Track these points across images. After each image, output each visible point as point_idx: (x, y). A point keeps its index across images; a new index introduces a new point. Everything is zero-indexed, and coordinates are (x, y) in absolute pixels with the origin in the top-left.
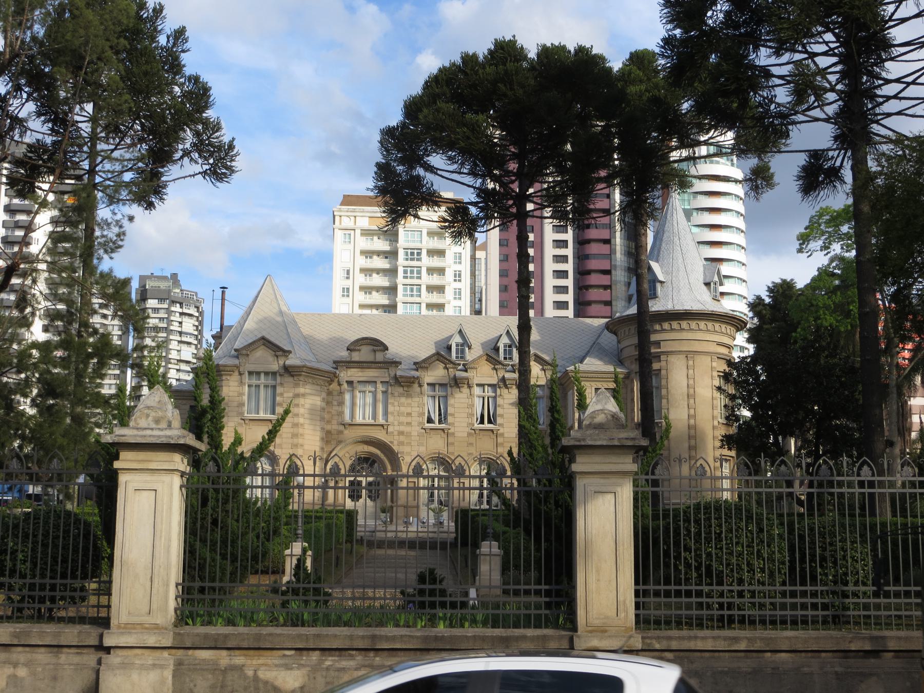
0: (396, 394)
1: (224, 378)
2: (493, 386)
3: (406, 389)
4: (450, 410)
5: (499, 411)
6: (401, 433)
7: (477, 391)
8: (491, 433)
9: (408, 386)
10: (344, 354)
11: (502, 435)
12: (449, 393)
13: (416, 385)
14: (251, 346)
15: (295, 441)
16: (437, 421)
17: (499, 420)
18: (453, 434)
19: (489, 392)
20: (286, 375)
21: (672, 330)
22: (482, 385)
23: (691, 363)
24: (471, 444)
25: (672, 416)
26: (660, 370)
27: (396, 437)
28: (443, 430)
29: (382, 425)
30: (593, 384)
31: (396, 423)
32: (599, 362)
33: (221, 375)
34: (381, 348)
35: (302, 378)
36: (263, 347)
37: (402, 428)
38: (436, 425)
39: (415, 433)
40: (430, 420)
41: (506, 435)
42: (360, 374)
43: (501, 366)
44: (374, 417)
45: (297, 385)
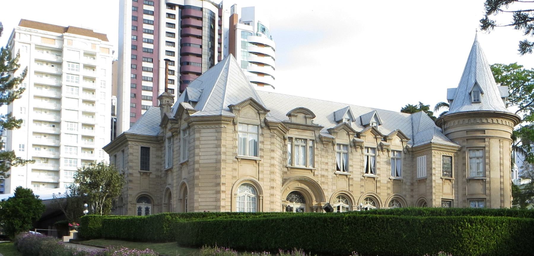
0: (319, 149)
1: (223, 126)
2: (373, 149)
3: (325, 146)
4: (350, 163)
5: (378, 166)
6: (323, 176)
7: (365, 151)
8: (373, 180)
9: (327, 144)
11: (380, 181)
12: (350, 151)
13: (331, 144)
15: (272, 176)
16: (342, 169)
17: (378, 172)
18: (352, 179)
19: (371, 153)
20: (265, 128)
22: (368, 148)
24: (362, 186)
25: (492, 176)
26: (485, 147)
27: (320, 179)
28: (346, 176)
29: (311, 170)
30: (441, 152)
31: (320, 169)
32: (440, 139)
33: (221, 124)
34: (311, 116)
35: (275, 132)
36: (249, 106)
37: (324, 173)
38: (341, 172)
39: (330, 177)
41: (381, 182)
42: (297, 133)
43: (379, 136)
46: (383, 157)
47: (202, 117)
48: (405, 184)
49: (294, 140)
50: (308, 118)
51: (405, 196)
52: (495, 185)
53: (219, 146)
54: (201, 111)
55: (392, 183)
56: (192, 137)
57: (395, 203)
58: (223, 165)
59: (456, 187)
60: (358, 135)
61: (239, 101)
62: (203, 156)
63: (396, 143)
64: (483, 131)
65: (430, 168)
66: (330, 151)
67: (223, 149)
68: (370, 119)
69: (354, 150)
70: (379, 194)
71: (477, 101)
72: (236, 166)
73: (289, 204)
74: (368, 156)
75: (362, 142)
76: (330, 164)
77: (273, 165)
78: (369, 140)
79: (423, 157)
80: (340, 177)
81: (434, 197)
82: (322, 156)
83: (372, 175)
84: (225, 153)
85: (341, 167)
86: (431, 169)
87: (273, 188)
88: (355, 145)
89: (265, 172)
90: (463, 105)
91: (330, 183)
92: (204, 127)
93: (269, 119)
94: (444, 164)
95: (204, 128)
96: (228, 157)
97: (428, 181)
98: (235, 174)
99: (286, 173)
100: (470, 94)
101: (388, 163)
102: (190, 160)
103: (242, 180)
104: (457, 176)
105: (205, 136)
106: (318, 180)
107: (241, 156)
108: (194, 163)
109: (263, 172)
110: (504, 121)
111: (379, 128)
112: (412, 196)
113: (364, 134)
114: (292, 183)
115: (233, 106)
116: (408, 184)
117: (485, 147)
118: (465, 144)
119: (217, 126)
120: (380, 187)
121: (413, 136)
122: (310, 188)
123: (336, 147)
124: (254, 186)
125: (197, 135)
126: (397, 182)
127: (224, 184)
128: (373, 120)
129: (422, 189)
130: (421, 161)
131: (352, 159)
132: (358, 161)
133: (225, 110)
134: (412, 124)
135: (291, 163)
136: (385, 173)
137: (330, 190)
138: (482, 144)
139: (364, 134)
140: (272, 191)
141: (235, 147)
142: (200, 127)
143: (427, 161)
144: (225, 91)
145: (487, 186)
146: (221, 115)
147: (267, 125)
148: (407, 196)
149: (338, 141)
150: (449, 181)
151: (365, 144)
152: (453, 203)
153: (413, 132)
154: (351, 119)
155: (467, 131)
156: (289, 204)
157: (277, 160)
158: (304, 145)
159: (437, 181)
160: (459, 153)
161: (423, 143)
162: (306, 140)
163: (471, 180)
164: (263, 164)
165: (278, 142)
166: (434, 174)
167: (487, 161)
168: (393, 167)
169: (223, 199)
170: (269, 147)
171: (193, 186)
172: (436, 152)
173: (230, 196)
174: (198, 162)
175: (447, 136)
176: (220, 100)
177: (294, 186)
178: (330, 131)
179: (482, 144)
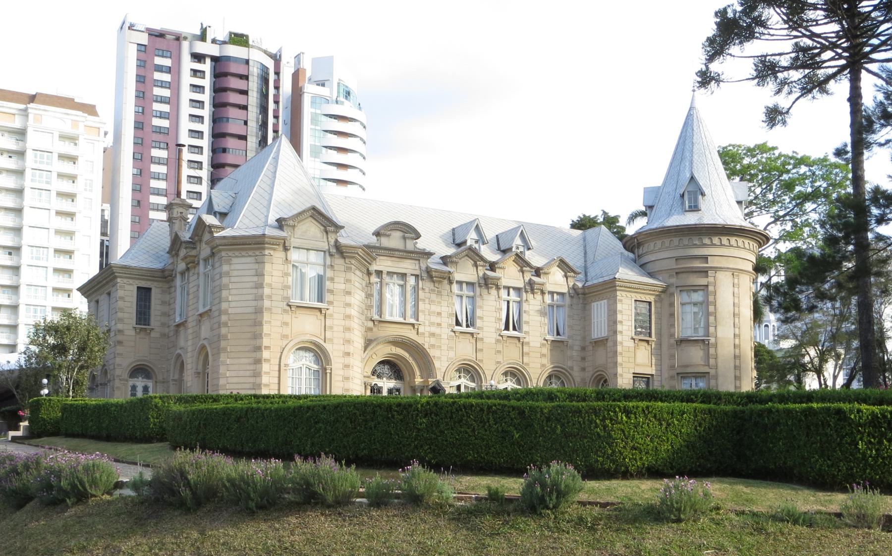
0: (427, 290)
1: (267, 252)
2: (518, 290)
3: (437, 285)
4: (479, 313)
5: (525, 317)
6: (433, 335)
7: (503, 293)
9: (440, 282)
10: (374, 240)
11: (528, 343)
12: (478, 293)
13: (446, 282)
14: (299, 216)
16: (464, 324)
17: (525, 328)
18: (482, 339)
19: (513, 296)
20: (336, 256)
21: (722, 245)
22: (508, 288)
23: (736, 281)
24: (499, 352)
25: (720, 334)
26: (707, 286)
27: (427, 339)
28: (472, 334)
29: (413, 325)
30: (633, 295)
31: (427, 324)
32: (631, 273)
33: (264, 249)
34: (413, 235)
35: (353, 261)
36: (311, 219)
37: (434, 329)
38: (464, 328)
39: (444, 336)
40: (458, 323)
41: (531, 344)
43: (528, 269)
44: (404, 315)
45: (348, 269)
46: (534, 304)
47: (234, 237)
48: (572, 348)
49: (384, 276)
50: (408, 238)
51: (572, 368)
52: (725, 350)
53: (259, 286)
54: (232, 227)
55: (548, 347)
56: (217, 271)
57: (553, 380)
58: (266, 317)
59: (658, 353)
60: (492, 266)
61: (295, 212)
62: (235, 301)
63: (556, 281)
64: (705, 258)
65: (613, 322)
66: (445, 293)
67: (267, 291)
68: (513, 239)
69: (485, 291)
70: (528, 364)
71: (695, 208)
72: (287, 318)
73: (375, 381)
74: (508, 302)
75: (499, 279)
76: (444, 314)
77: (348, 317)
78: (510, 275)
79: (602, 302)
80: (461, 336)
81: (619, 370)
82: (431, 302)
83: (515, 334)
84: (270, 297)
85: (462, 319)
86: (615, 322)
87: (348, 354)
88: (487, 283)
89: (335, 329)
90: (670, 215)
91: (444, 347)
92: (237, 253)
93: (342, 240)
94: (637, 314)
95: (236, 257)
96: (274, 304)
97: (610, 344)
98: (286, 331)
99: (370, 329)
100: (682, 196)
101: (542, 313)
102: (214, 308)
103: (296, 341)
104: (659, 335)
105: (238, 268)
106: (424, 341)
107: (296, 301)
108: (220, 313)
109: (331, 328)
110: (740, 240)
111: (529, 256)
112: (583, 369)
113: (501, 265)
114: (379, 347)
115: (284, 219)
116: (577, 348)
117: (707, 286)
118: (673, 280)
119: (257, 253)
120: (528, 354)
121: (586, 268)
122: (411, 355)
123: (455, 287)
124: (319, 353)
125: (225, 268)
126: (557, 346)
127: (267, 348)
128: (518, 241)
129: (600, 357)
130: (599, 309)
131: (481, 307)
132: (492, 310)
133: (271, 226)
134: (585, 247)
135: (380, 313)
136: (537, 330)
137: (444, 358)
138: (703, 281)
139: (501, 265)
140: (347, 360)
141: (286, 287)
142: (230, 254)
143: (609, 310)
144: (271, 195)
145: (712, 351)
146: (264, 235)
147: (340, 250)
148: (576, 368)
149: (457, 277)
150: (646, 344)
151: (504, 282)
152: (653, 380)
153: (585, 261)
154: (481, 240)
155: (677, 259)
156: (375, 381)
157: (356, 308)
158: (402, 283)
159: (625, 344)
160: (663, 296)
161: (601, 280)
162: (406, 274)
163: (682, 341)
164: (331, 315)
165: (357, 279)
166: (621, 332)
167: (711, 309)
168: (551, 320)
169: (266, 373)
170: (343, 286)
171: (218, 351)
172: (624, 294)
173: (277, 368)
174: (226, 312)
175: (644, 268)
176: (264, 210)
177: (384, 351)
178: (445, 260)
179: (703, 281)
